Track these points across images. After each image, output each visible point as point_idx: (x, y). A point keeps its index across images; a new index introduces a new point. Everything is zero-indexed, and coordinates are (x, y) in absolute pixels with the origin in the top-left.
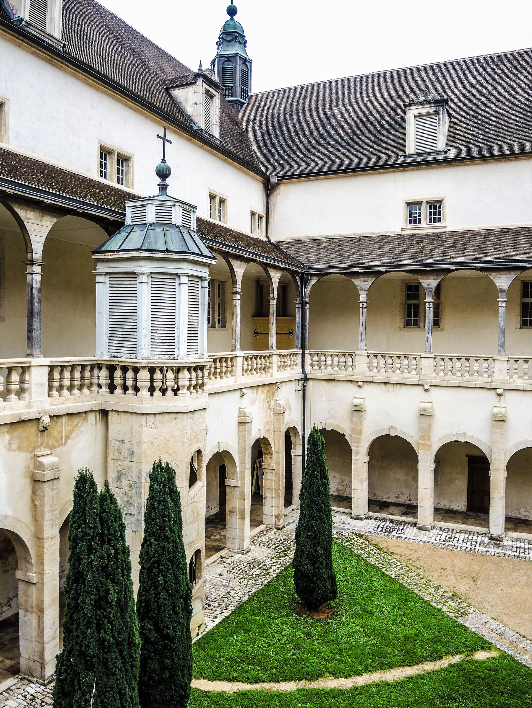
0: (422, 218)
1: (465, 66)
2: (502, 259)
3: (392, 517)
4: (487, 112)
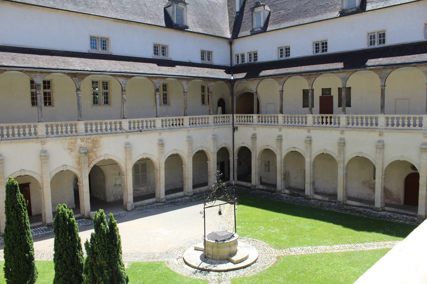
2: (36, 66)
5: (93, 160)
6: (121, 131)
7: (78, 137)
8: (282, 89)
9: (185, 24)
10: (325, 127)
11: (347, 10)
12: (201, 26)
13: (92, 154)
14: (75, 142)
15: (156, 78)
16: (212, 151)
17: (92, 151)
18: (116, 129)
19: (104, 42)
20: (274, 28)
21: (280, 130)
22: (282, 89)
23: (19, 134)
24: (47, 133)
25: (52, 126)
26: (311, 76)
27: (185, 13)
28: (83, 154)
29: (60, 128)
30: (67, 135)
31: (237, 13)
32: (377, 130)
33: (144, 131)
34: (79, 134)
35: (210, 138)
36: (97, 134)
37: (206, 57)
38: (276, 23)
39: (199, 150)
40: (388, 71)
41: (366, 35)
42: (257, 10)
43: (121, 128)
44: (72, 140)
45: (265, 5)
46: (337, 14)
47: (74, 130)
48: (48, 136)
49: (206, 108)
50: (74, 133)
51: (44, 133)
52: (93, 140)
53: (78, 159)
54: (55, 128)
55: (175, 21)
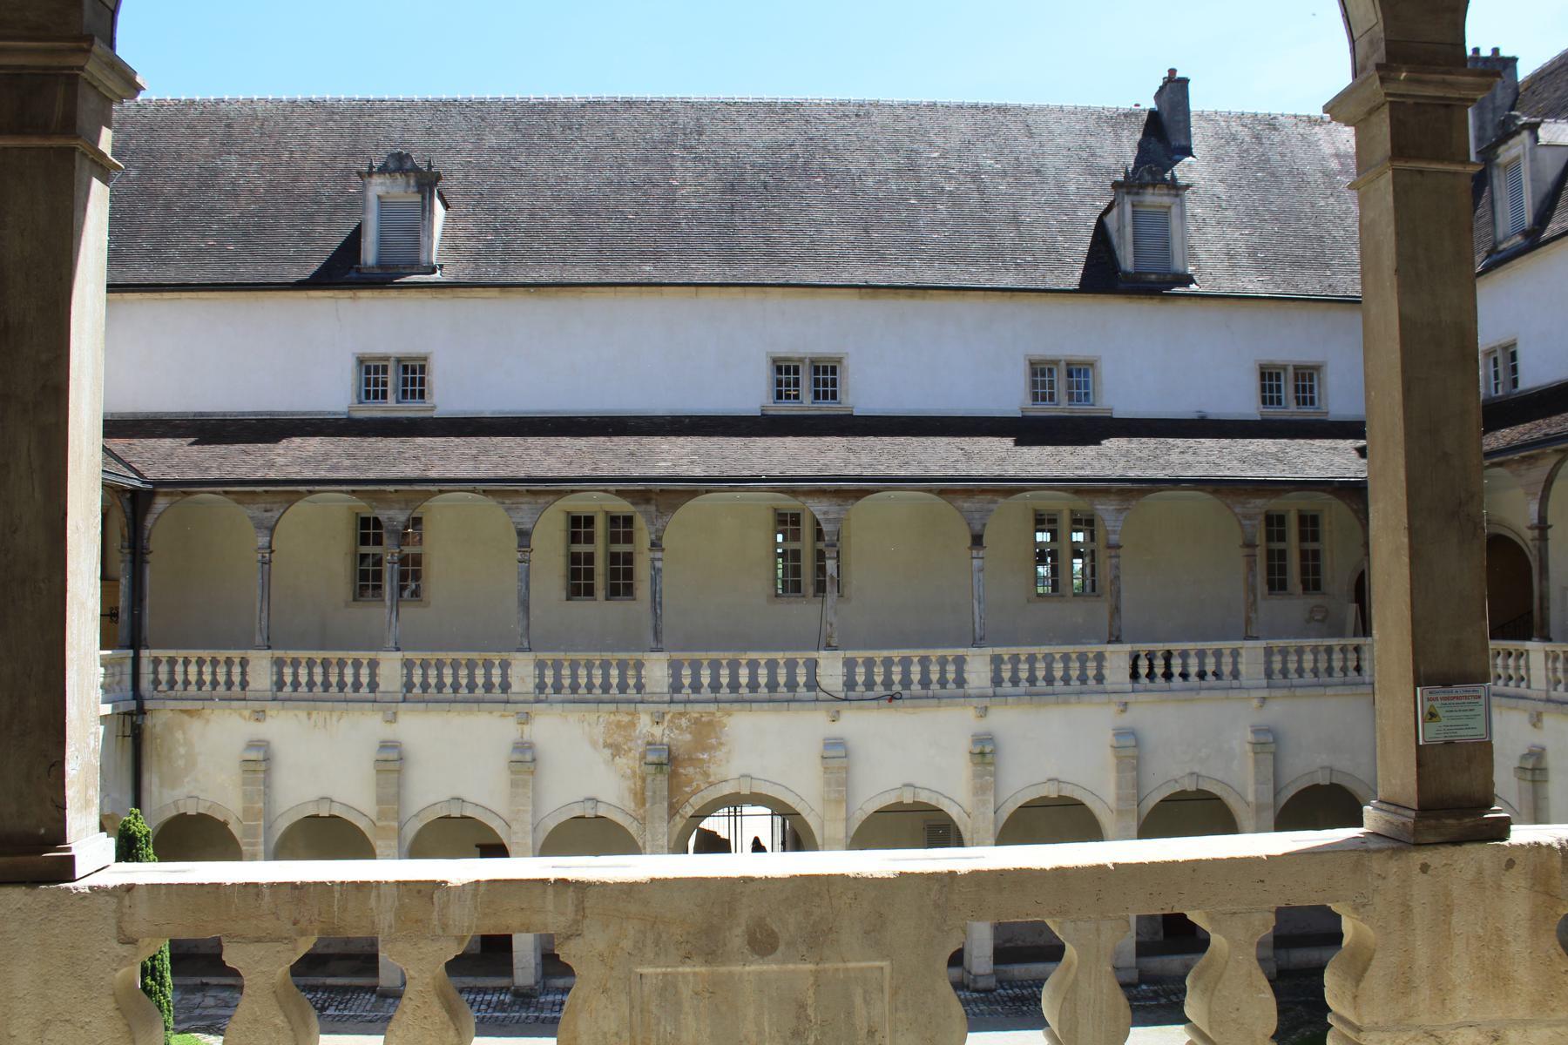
0: (390, 388)
1: (478, 113)
2: (522, 475)
3: (330, 981)
4: (514, 202)
5: (694, 793)
6: (812, 694)
7: (640, 706)
8: (1542, 518)
12: (1263, 266)
13: (691, 770)
14: (633, 724)
15: (969, 492)
16: (1251, 798)
17: (691, 759)
18: (792, 685)
19: (826, 374)
21: (1536, 721)
22: (1542, 518)
23: (456, 687)
24: (541, 687)
25: (557, 665)
27: (1175, 223)
28: (652, 769)
29: (582, 672)
30: (605, 696)
34: (646, 697)
35: (1240, 740)
36: (716, 701)
37: (1288, 390)
39: (1178, 789)
42: (1506, 153)
43: (813, 684)
44: (619, 717)
45: (1538, 125)
47: (631, 682)
48: (542, 697)
49: (1295, 605)
50: (632, 692)
51: (530, 685)
52: (697, 721)
53: (639, 783)
54: (566, 672)
55: (1127, 260)
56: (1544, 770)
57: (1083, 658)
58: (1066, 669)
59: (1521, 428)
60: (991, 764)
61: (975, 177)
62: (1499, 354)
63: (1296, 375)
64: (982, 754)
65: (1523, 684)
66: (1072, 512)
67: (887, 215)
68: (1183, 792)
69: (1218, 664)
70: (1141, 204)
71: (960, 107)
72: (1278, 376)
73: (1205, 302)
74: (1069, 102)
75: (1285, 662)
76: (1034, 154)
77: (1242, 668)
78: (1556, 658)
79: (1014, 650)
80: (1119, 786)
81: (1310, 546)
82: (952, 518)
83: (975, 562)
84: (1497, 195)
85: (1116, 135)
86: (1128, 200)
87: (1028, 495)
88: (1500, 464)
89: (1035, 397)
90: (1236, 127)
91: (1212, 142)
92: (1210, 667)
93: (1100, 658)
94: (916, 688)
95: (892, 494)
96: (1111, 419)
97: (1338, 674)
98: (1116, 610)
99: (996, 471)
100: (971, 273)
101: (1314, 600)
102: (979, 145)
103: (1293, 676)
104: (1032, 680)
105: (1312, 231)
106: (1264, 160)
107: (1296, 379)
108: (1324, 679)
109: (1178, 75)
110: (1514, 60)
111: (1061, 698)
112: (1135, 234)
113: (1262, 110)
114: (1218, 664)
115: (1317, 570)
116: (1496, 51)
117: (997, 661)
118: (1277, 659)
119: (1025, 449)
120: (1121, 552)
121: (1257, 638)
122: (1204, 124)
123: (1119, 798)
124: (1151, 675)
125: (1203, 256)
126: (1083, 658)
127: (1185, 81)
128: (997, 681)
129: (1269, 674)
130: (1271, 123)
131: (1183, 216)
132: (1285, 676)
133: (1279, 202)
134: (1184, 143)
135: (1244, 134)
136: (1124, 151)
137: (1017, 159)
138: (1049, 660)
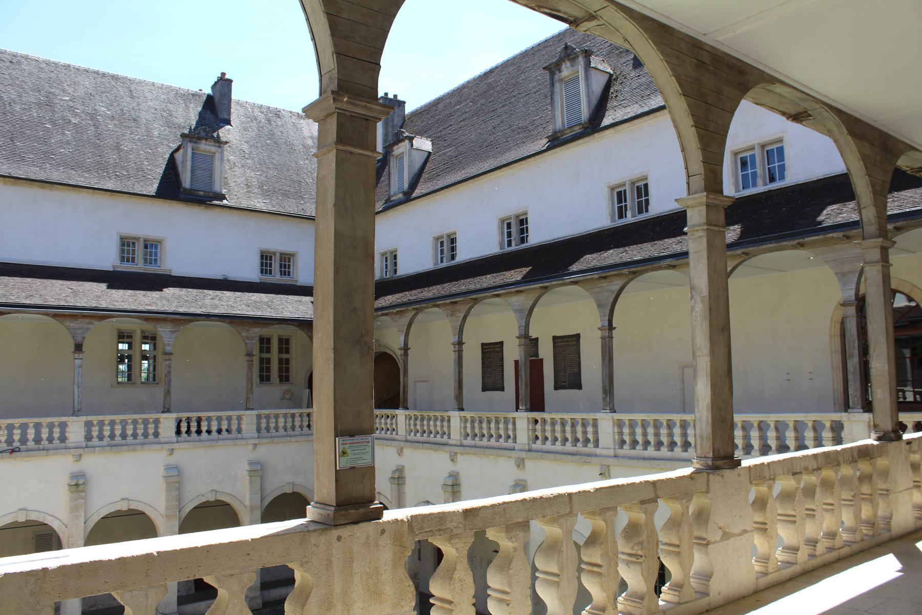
8: (406, 344)
9: (217, 188)
10: (487, 447)
11: (562, 132)
12: (265, 194)
15: (74, 317)
16: (247, 503)
20: (424, 191)
21: (400, 452)
22: (406, 344)
26: (458, 307)
27: (217, 163)
31: (379, 161)
32: (594, 459)
33: (28, 450)
35: (241, 469)
37: (276, 267)
38: (431, 179)
39: (204, 500)
40: (616, 284)
41: (606, 192)
45: (413, 138)
46: (543, 143)
49: (275, 390)
55: (186, 182)
56: (403, 478)
57: (146, 422)
58: (135, 429)
59: (397, 296)
60: (82, 491)
61: (93, 117)
62: (388, 255)
63: (281, 258)
64: (77, 485)
65: (394, 433)
66: (142, 331)
67: (28, 132)
68: (208, 502)
69: (229, 424)
70: (197, 149)
71: (87, 71)
72: (271, 257)
73: (231, 211)
74: (159, 81)
75: (268, 423)
76: (133, 109)
77: (243, 427)
78: (410, 419)
79: (101, 418)
80: (167, 501)
81: (284, 356)
82: (62, 333)
83: (77, 362)
84: (392, 171)
85: (186, 105)
86: (190, 147)
87: (114, 320)
88: (386, 314)
89: (123, 259)
90: (257, 113)
91: (243, 119)
92: (224, 427)
93: (157, 422)
94: (31, 444)
95: (20, 315)
96: (170, 276)
97: (298, 429)
98: (168, 393)
99: (94, 304)
100: (85, 177)
101: (285, 387)
102: (97, 97)
103: (273, 430)
104: (112, 436)
105: (295, 177)
106: (271, 135)
107: (281, 261)
108: (290, 432)
109: (227, 77)
110: (404, 103)
111: (131, 447)
112: (192, 166)
113: (273, 105)
114: (229, 424)
115: (287, 370)
116: (395, 96)
117: (89, 425)
118: (264, 421)
119: (114, 291)
120: (172, 357)
121: (252, 409)
122: (239, 108)
123: (167, 508)
124: (188, 432)
125: (232, 184)
126: (146, 422)
127: (230, 81)
128: (89, 438)
129: (259, 430)
130: (277, 114)
131: (222, 160)
132: (268, 431)
133: (278, 158)
134: (226, 117)
135: (261, 117)
136: (191, 116)
137: (122, 110)
138: (124, 423)
